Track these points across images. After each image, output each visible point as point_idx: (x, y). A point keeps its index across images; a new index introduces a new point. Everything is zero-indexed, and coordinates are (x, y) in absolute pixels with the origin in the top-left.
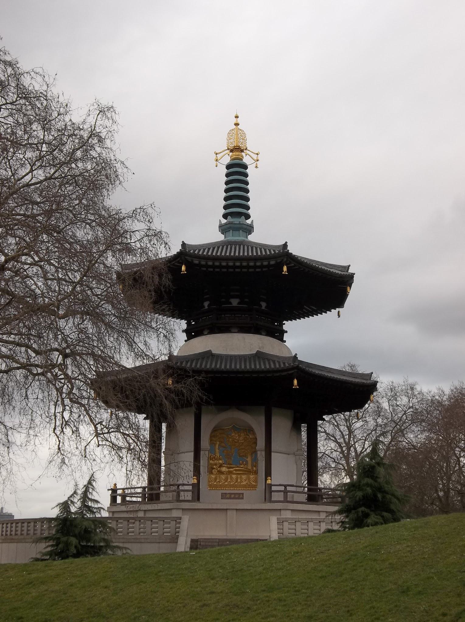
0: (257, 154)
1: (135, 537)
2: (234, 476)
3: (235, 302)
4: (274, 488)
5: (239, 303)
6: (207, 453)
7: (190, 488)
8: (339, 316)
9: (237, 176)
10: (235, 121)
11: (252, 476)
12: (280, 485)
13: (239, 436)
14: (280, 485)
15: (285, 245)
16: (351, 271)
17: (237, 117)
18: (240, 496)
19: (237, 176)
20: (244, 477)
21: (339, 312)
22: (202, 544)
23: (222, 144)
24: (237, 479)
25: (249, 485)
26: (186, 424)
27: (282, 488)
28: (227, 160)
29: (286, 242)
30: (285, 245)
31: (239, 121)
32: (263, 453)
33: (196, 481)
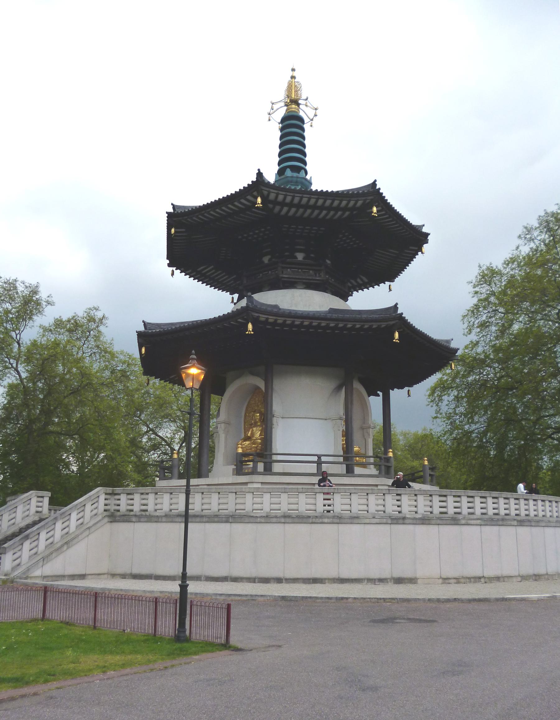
0: (316, 109)
3: (300, 256)
5: (304, 258)
8: (390, 290)
9: (292, 130)
10: (291, 73)
15: (374, 184)
16: (424, 230)
17: (293, 70)
19: (292, 130)
21: (390, 286)
23: (280, 95)
28: (281, 113)
29: (375, 181)
30: (374, 184)
31: (295, 74)
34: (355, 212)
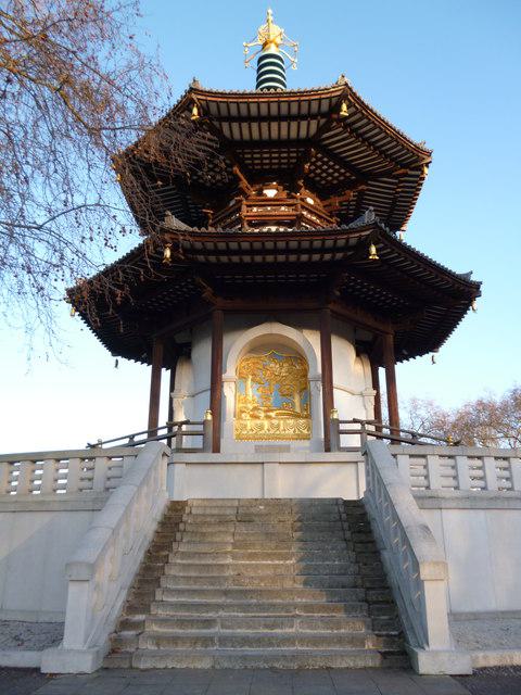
1: (41, 499)
2: (275, 422)
4: (343, 427)
6: (233, 385)
7: (200, 428)
11: (302, 421)
12: (355, 421)
13: (282, 367)
14: (355, 421)
18: (287, 449)
20: (291, 422)
22: (194, 512)
24: (279, 425)
25: (298, 435)
26: (202, 352)
27: (358, 427)
32: (320, 385)
33: (209, 417)
34: (323, 121)
